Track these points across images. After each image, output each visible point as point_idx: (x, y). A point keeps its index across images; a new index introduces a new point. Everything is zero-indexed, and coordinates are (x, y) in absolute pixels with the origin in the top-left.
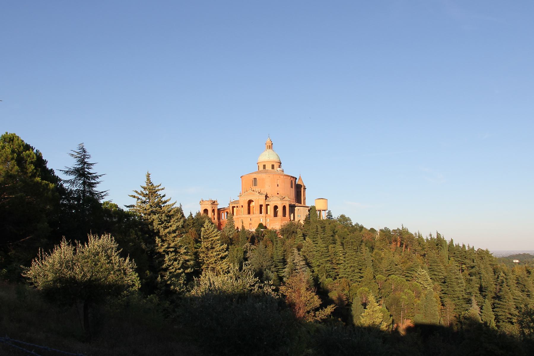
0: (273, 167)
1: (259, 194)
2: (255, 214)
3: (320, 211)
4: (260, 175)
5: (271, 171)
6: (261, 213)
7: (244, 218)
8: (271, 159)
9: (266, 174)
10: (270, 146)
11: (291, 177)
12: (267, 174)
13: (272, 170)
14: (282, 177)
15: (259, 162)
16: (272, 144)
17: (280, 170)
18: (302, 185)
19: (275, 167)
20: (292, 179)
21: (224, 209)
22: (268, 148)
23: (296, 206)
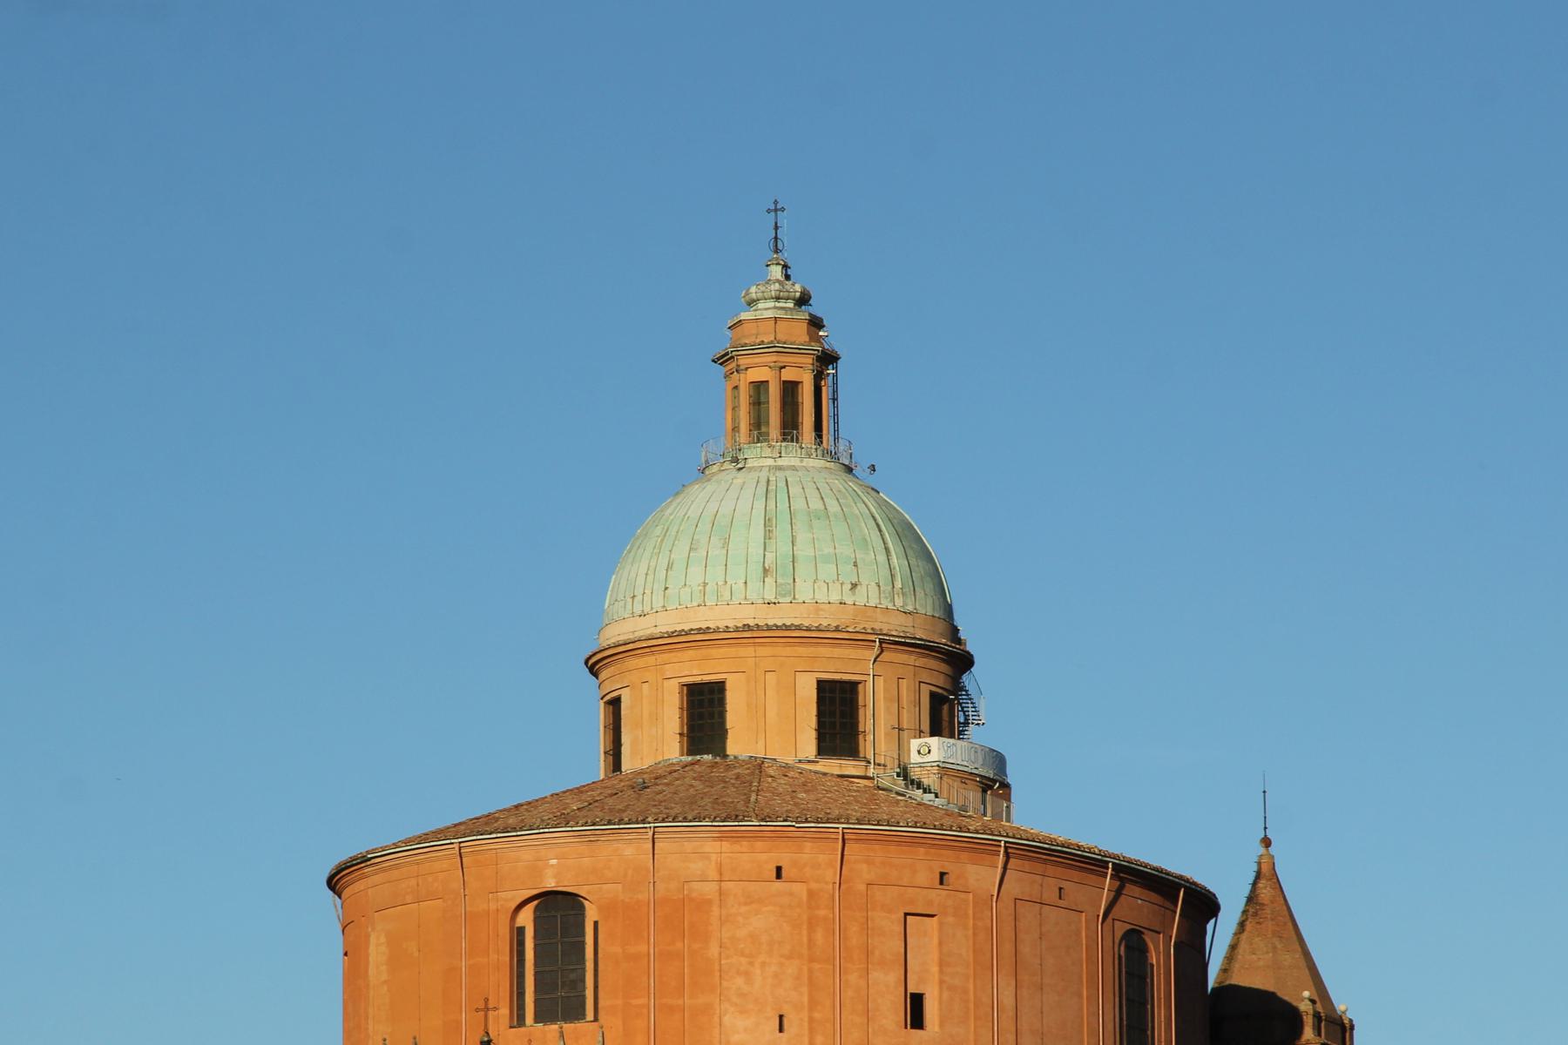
5: (808, 783)
8: (804, 592)
11: (1131, 875)
12: (755, 836)
13: (834, 766)
14: (982, 876)
15: (614, 634)
17: (944, 770)
19: (865, 722)
20: (1138, 906)
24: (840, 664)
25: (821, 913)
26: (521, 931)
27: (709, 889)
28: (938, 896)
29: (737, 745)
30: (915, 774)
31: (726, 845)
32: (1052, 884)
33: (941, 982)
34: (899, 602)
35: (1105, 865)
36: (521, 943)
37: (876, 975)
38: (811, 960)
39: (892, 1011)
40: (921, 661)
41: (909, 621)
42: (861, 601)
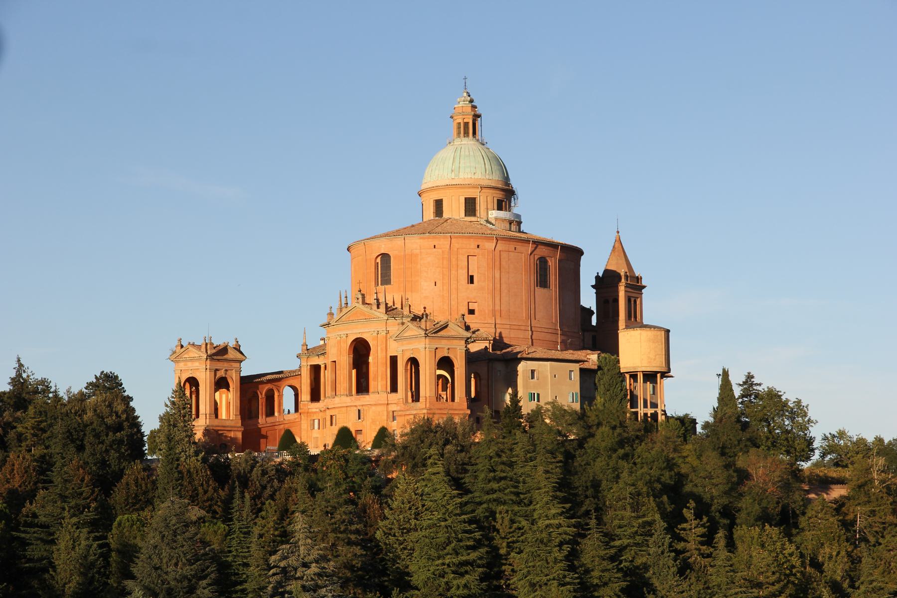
0: (470, 206)
1: (386, 317)
2: (373, 392)
3: (634, 376)
4: (399, 241)
6: (394, 389)
7: (337, 410)
9: (421, 238)
10: (466, 124)
12: (428, 238)
14: (490, 245)
15: (424, 187)
16: (479, 116)
17: (496, 219)
18: (622, 274)
20: (542, 251)
21: (278, 378)
22: (459, 133)
23: (520, 360)
24: (471, 193)
25: (445, 256)
26: (378, 263)
27: (418, 251)
28: (478, 249)
29: (446, 215)
30: (490, 220)
31: (421, 240)
32: (512, 247)
33: (478, 272)
34: (487, 177)
35: (530, 241)
36: (378, 266)
37: (460, 271)
38: (443, 268)
39: (464, 278)
40: (494, 191)
41: (490, 181)
42: (476, 177)
